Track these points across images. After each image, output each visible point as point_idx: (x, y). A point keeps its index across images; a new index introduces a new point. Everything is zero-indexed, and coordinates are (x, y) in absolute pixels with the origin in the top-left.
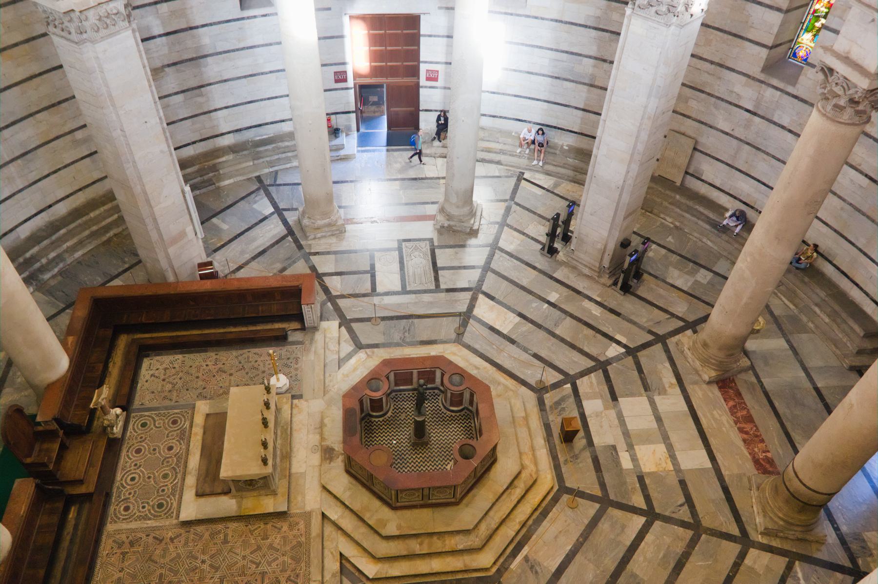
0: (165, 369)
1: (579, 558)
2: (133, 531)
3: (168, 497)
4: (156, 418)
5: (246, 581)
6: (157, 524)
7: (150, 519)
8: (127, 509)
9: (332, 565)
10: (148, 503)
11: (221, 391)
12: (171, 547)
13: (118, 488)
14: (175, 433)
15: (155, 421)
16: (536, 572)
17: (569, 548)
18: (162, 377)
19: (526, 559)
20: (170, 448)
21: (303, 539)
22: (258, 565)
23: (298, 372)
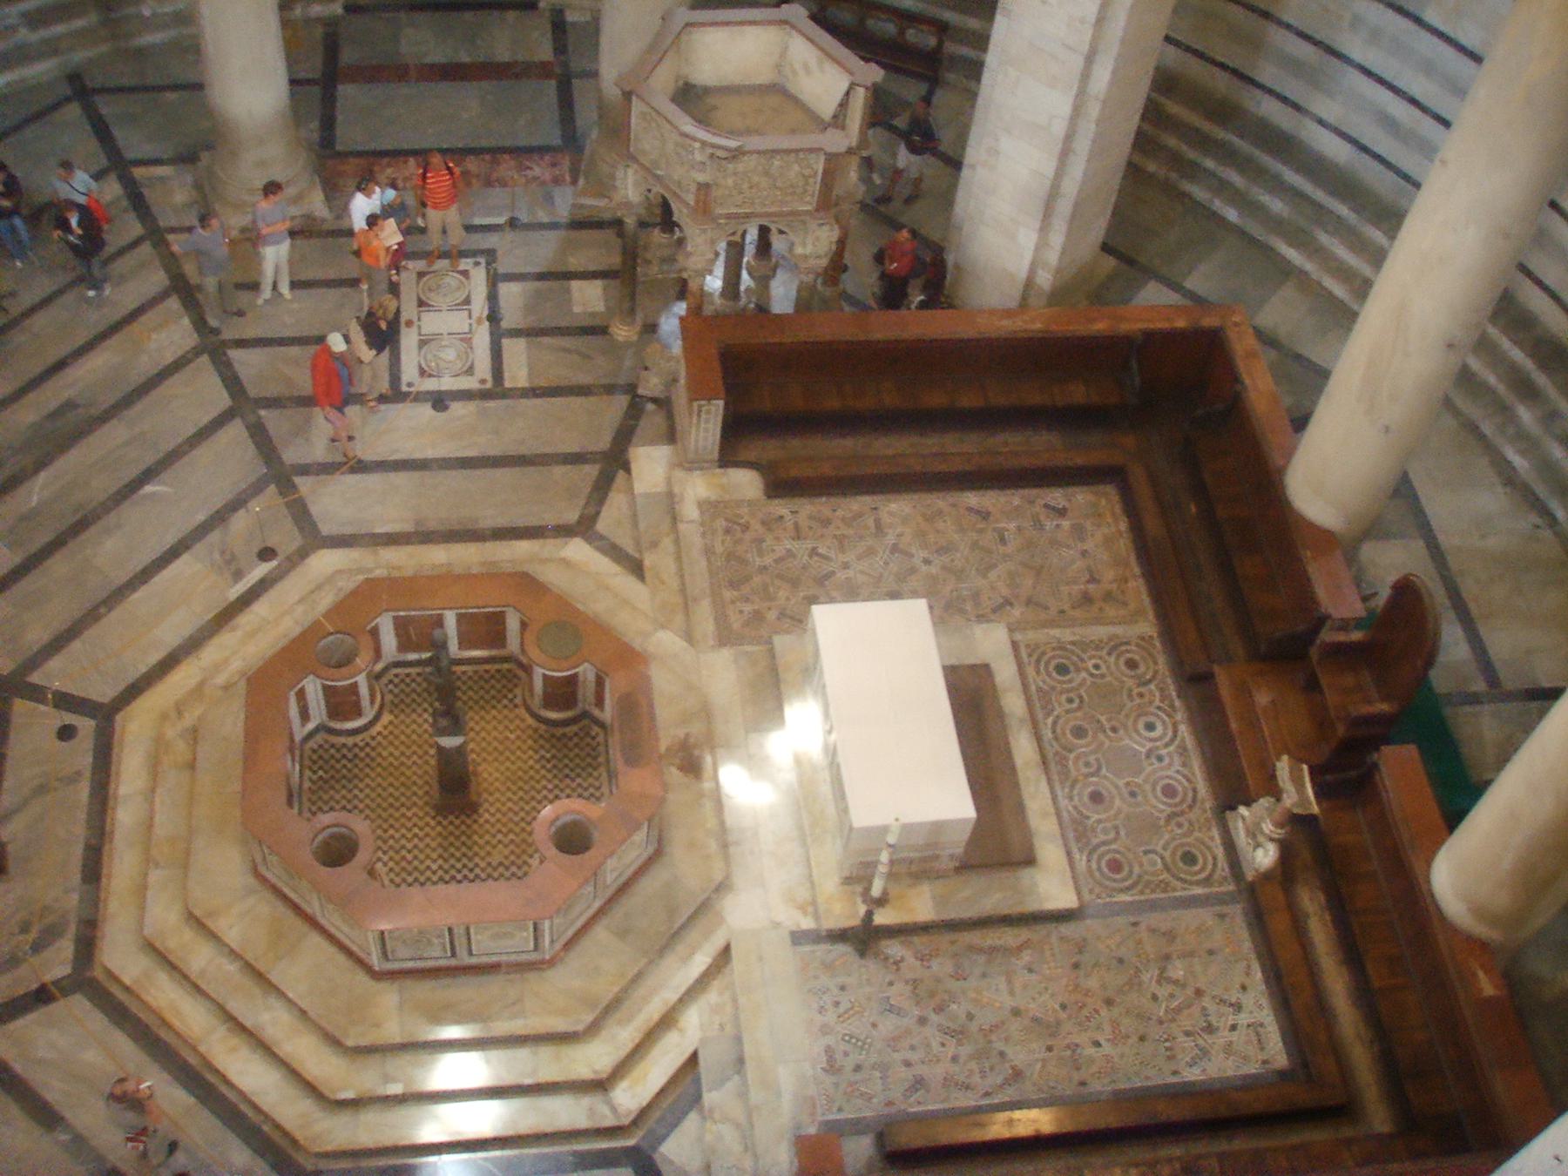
0: (1210, 1029)
1: (122, 577)
2: (1098, 621)
3: (1053, 688)
4: (1165, 876)
5: (832, 527)
6: (1056, 632)
7: (1073, 643)
8: (1132, 664)
9: (659, 561)
10: (1092, 675)
11: (1026, 956)
12: (1005, 591)
13: (1172, 706)
14: (1102, 837)
15: (1167, 868)
16: (223, 553)
17: (136, 596)
18: (1206, 1002)
19: (238, 575)
20: (1096, 797)
21: (728, 594)
22: (813, 552)
23: (819, 1019)
